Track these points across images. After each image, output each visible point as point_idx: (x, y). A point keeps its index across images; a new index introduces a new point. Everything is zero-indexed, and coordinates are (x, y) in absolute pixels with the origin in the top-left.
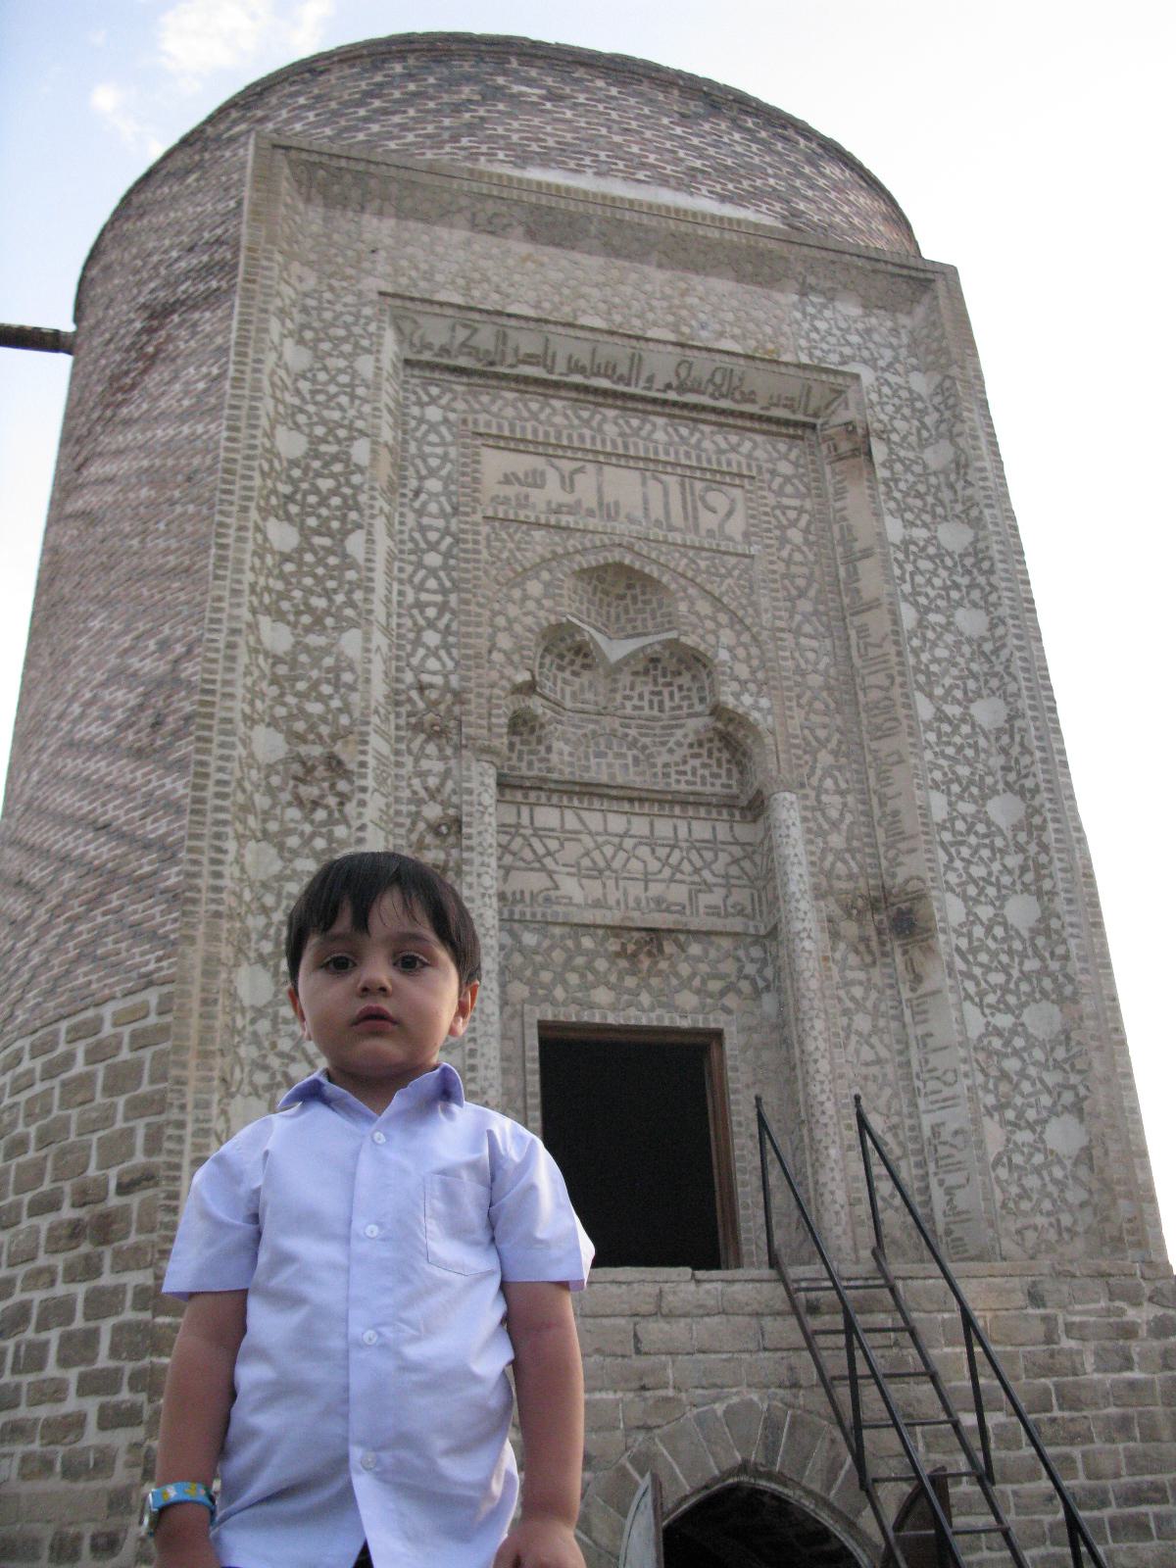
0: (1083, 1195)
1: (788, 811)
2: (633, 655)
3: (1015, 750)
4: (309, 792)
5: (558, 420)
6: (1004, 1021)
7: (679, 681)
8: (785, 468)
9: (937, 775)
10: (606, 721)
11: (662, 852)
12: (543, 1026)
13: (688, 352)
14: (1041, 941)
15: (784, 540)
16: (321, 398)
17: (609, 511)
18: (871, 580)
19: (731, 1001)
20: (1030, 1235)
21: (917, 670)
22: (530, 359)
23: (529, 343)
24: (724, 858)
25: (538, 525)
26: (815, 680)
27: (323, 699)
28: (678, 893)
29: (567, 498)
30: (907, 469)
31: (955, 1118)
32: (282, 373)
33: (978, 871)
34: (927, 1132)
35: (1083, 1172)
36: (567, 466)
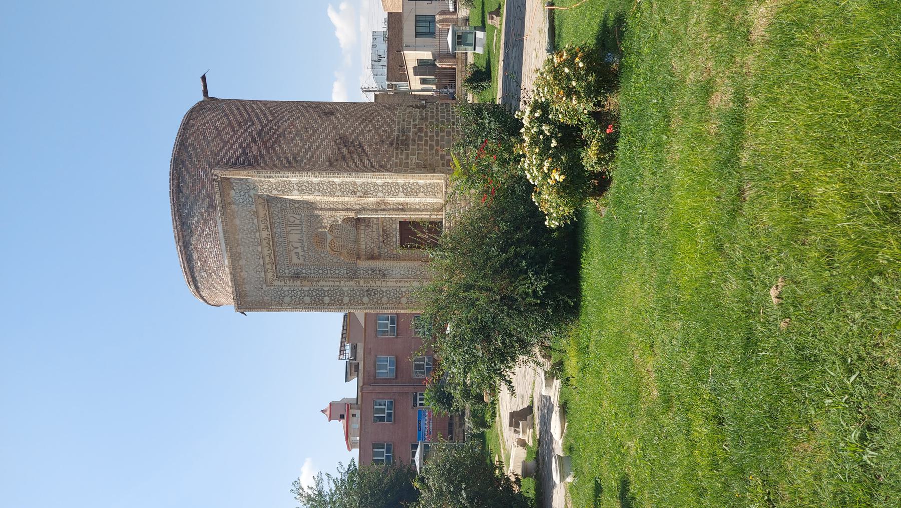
8: (279, 205)
17: (301, 241)
23: (267, 259)
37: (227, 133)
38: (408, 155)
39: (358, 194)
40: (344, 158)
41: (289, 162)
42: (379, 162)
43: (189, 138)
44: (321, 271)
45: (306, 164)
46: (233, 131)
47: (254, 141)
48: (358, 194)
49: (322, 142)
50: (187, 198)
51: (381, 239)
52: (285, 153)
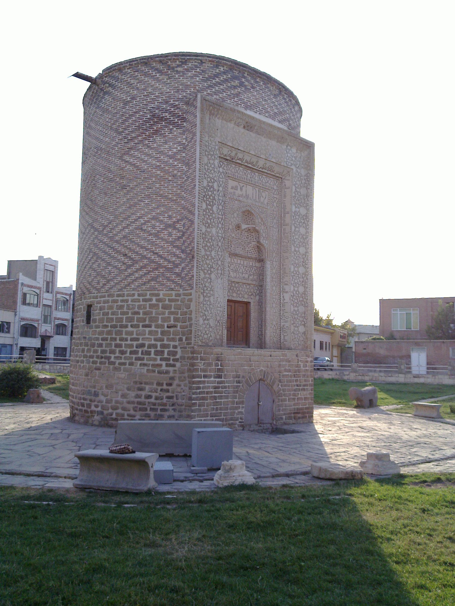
0: (303, 339)
1: (268, 265)
2: (246, 228)
3: (305, 259)
6: (296, 309)
7: (252, 234)
8: (275, 187)
9: (293, 262)
10: (239, 240)
11: (245, 267)
13: (267, 161)
14: (303, 295)
16: (209, 171)
17: (247, 197)
18: (288, 219)
19: (252, 297)
20: (295, 345)
21: (293, 240)
23: (240, 155)
24: (254, 270)
26: (275, 238)
27: (210, 242)
28: (246, 276)
29: (240, 193)
31: (287, 324)
34: (282, 326)
35: (303, 335)
36: (242, 185)
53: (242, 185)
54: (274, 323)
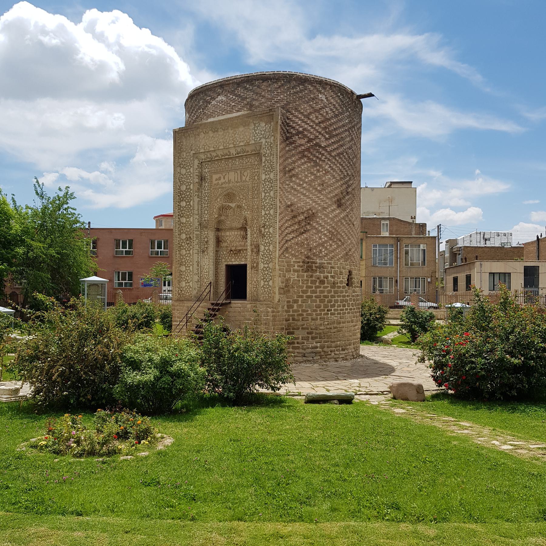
4: (188, 242)
5: (223, 165)
6: (266, 266)
8: (256, 163)
12: (226, 265)
15: (254, 179)
17: (229, 181)
22: (216, 157)
23: (214, 154)
25: (219, 188)
26: (256, 207)
29: (224, 181)
30: (268, 162)
32: (181, 176)
33: (267, 241)
37: (317, 117)
38: (297, 271)
39: (263, 229)
40: (295, 217)
41: (290, 171)
42: (291, 247)
43: (312, 86)
44: (206, 198)
45: (288, 185)
46: (320, 123)
47: (310, 140)
48: (263, 229)
49: (310, 198)
50: (259, 87)
51: (233, 249)
52: (299, 167)
53: (224, 174)
54: (255, 279)
